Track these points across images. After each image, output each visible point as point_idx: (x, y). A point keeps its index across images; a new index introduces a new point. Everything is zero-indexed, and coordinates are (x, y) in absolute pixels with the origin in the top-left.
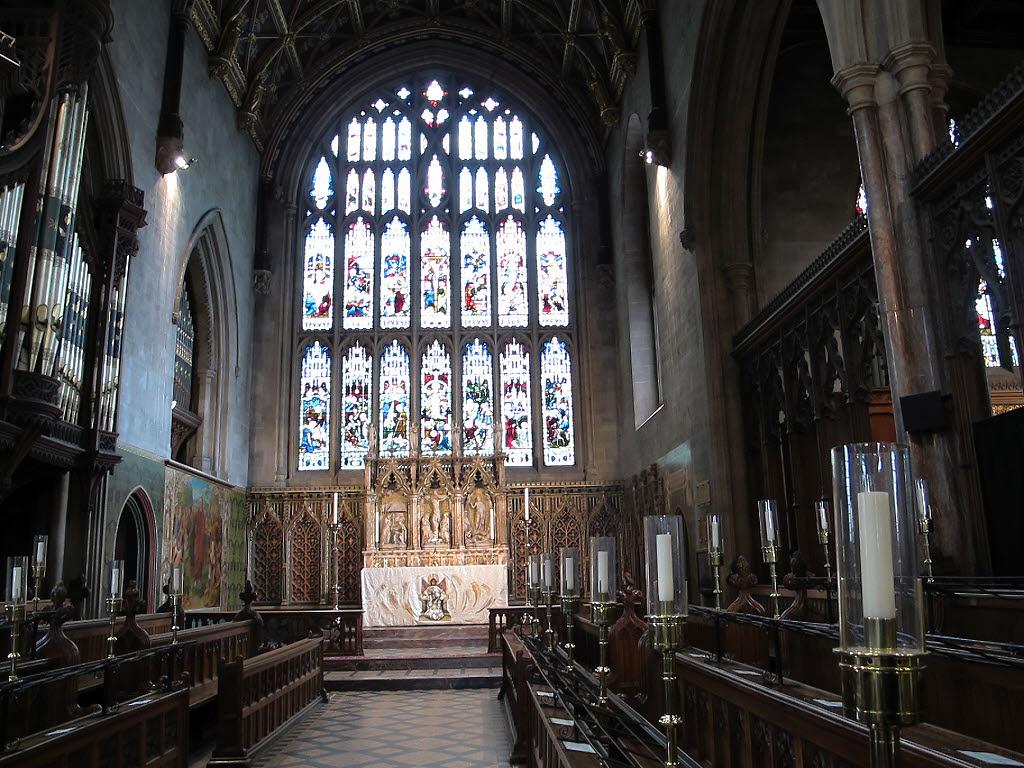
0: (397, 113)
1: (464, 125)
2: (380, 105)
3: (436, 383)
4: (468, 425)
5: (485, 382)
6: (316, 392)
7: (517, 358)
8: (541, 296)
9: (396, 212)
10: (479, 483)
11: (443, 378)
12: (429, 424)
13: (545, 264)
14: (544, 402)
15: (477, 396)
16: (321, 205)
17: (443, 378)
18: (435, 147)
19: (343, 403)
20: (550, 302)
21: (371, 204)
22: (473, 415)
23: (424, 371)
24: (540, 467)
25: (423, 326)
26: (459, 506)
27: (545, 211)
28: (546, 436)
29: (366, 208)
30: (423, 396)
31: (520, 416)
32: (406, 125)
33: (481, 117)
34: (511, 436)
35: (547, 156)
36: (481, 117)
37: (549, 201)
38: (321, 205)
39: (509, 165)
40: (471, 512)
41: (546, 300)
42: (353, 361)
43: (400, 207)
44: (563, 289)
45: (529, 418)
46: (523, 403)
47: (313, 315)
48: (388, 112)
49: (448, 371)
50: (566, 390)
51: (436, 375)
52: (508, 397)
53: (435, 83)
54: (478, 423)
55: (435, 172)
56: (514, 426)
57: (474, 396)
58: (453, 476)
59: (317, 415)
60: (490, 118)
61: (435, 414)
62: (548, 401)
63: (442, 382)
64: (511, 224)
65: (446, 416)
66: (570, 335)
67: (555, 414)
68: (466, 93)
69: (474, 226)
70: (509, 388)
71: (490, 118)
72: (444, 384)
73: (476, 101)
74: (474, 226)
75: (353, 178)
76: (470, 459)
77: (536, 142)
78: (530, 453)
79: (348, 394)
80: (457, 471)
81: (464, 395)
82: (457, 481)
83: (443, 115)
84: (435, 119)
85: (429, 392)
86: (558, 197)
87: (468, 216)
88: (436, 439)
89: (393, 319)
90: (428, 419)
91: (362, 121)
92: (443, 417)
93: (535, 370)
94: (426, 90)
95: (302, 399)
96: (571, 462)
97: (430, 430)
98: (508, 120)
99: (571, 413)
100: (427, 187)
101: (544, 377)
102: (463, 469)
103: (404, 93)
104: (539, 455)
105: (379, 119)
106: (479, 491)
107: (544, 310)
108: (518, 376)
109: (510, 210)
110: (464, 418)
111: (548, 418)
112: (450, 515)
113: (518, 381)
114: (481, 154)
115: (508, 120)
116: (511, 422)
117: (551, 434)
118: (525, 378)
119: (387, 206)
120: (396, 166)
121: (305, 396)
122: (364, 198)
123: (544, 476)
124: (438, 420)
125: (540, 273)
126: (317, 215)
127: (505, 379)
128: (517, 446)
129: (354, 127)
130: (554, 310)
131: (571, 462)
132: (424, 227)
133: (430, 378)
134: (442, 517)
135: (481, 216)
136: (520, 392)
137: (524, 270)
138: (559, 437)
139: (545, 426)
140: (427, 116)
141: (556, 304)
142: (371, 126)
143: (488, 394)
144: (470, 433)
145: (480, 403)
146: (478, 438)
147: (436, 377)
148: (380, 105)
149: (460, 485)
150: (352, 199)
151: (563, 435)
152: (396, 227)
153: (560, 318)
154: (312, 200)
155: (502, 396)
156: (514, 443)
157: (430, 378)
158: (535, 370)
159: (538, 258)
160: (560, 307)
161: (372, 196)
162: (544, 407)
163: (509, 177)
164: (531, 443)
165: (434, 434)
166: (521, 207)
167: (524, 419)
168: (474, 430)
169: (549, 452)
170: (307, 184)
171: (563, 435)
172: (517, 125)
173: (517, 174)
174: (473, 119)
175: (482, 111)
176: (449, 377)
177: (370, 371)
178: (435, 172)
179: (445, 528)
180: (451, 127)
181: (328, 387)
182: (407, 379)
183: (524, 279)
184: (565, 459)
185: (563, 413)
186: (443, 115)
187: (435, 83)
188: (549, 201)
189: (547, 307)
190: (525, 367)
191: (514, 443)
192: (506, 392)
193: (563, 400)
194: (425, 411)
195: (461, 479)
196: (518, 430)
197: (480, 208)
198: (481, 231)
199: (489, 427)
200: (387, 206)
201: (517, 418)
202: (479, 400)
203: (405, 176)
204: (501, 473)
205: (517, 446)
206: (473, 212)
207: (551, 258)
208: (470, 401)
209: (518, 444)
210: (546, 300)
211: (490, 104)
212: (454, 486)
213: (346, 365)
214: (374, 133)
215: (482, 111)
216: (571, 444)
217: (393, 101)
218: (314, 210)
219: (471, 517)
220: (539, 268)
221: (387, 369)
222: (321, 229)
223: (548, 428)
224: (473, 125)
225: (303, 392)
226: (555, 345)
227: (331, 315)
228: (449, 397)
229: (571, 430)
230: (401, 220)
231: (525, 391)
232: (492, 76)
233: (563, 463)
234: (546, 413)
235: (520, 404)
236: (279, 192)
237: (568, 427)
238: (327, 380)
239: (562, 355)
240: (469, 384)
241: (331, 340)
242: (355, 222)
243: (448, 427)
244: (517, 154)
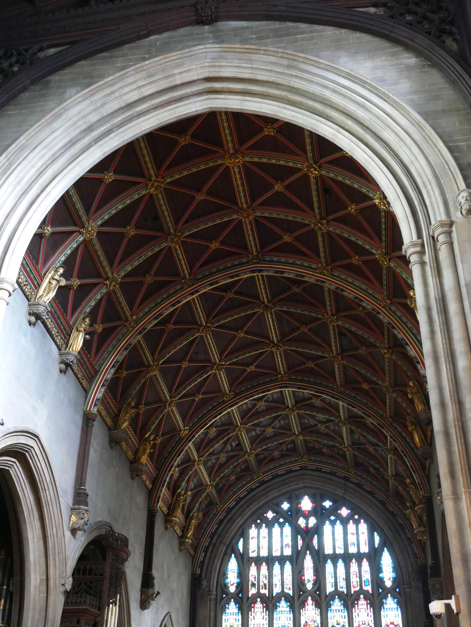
0: (281, 520)
1: (327, 528)
2: (270, 515)
9: (283, 594)
16: (232, 589)
18: (308, 546)
21: (266, 589)
29: (263, 591)
32: (287, 529)
33: (338, 522)
35: (385, 549)
36: (338, 522)
37: (388, 584)
38: (232, 589)
39: (359, 557)
43: (286, 591)
48: (275, 520)
53: (306, 497)
55: (308, 563)
60: (345, 522)
64: (362, 602)
68: (327, 504)
69: (337, 604)
71: (345, 522)
73: (334, 510)
74: (337, 604)
75: (253, 570)
77: (377, 539)
83: (312, 521)
84: (307, 524)
86: (395, 580)
87: (332, 597)
91: (258, 527)
94: (300, 503)
98: (357, 523)
100: (303, 575)
103: (285, 506)
105: (270, 525)
109: (361, 591)
114: (340, 551)
115: (357, 523)
119: (277, 590)
120: (282, 560)
122: (261, 584)
126: (230, 596)
129: (253, 532)
132: (303, 605)
135: (342, 596)
140: (302, 522)
142: (264, 531)
148: (270, 515)
150: (253, 585)
152: (283, 605)
154: (226, 586)
161: (266, 582)
163: (360, 566)
166: (368, 588)
170: (223, 574)
172: (363, 527)
173: (365, 564)
174: (333, 523)
175: (339, 517)
178: (308, 563)
180: (318, 530)
186: (312, 521)
187: (306, 497)
188: (388, 584)
197: (341, 590)
198: (342, 608)
200: (277, 590)
203: (288, 567)
206: (337, 593)
211: (344, 512)
214: (267, 535)
215: (339, 517)
217: (279, 512)
218: (228, 593)
222: (232, 608)
224: (333, 527)
230: (286, 601)
232: (344, 494)
236: (205, 583)
242: (255, 602)
244: (365, 549)
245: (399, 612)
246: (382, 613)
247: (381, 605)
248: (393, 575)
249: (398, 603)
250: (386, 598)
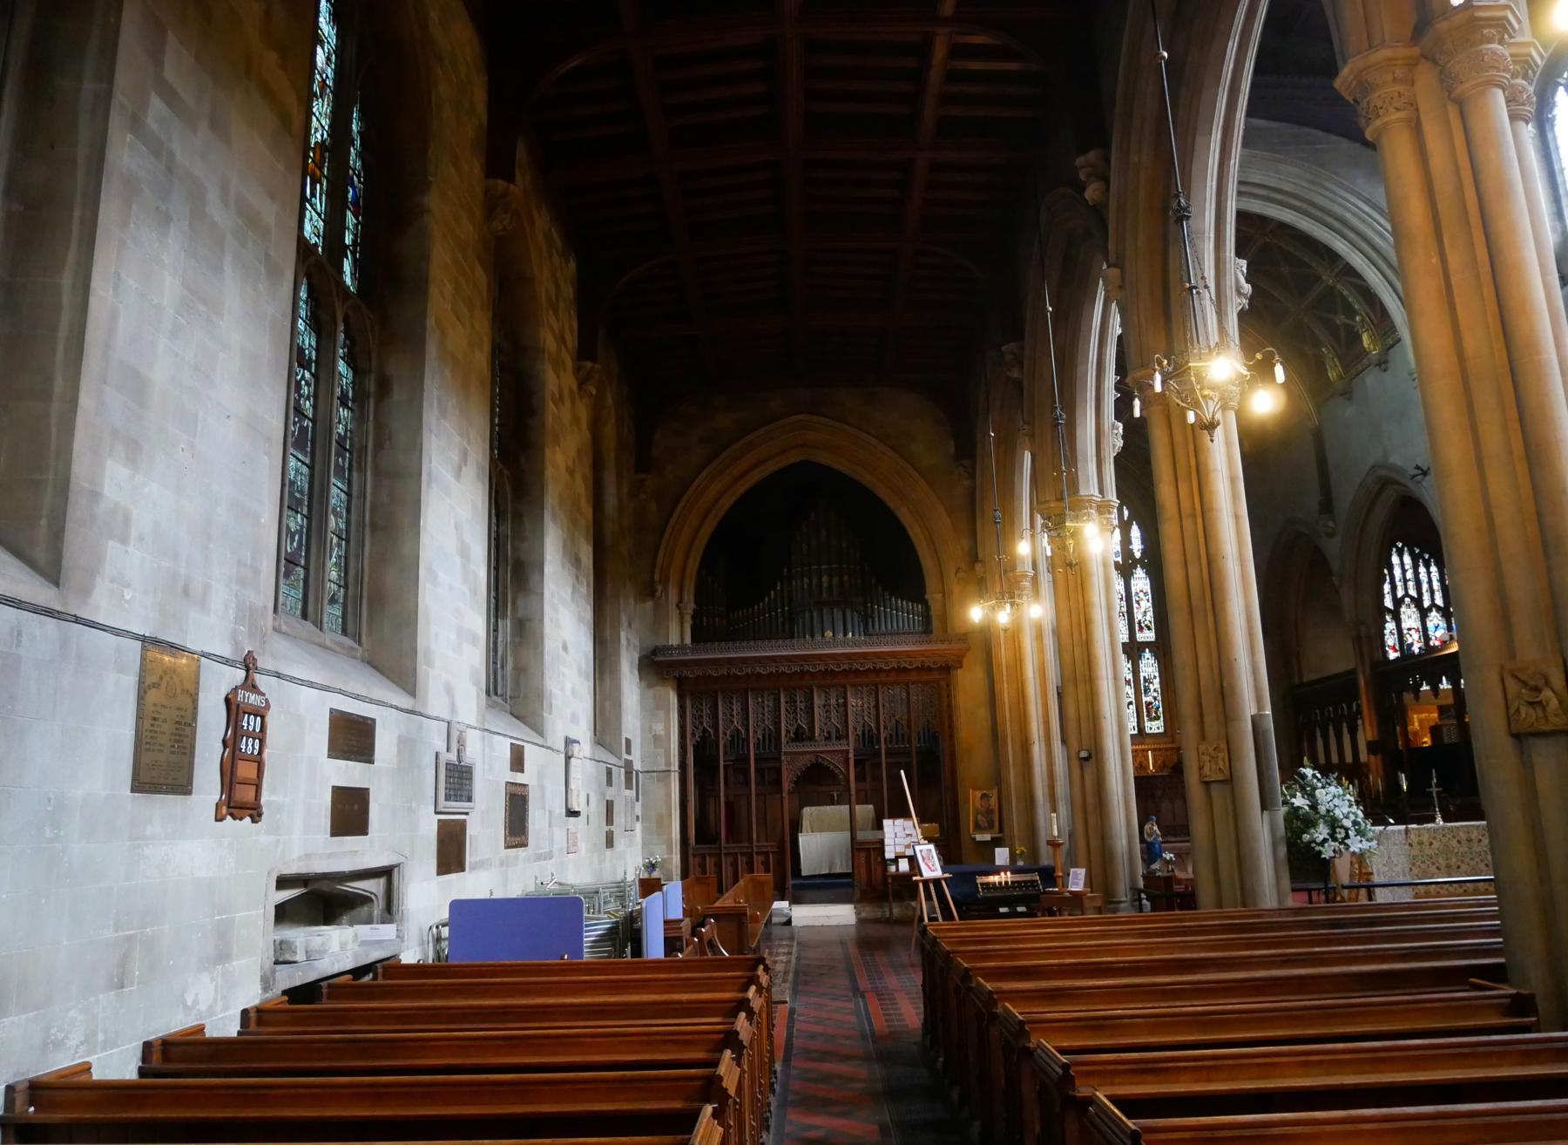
8: (1136, 621)
13: (1138, 599)
20: (1143, 625)
27: (1135, 562)
28: (1145, 714)
37: (1138, 555)
41: (1140, 623)
44: (1150, 616)
46: (1129, 693)
50: (1156, 684)
66: (1158, 648)
67: (1149, 699)
77: (1126, 513)
78: (1135, 724)
86: (1144, 552)
93: (1136, 671)
96: (1161, 730)
99: (1160, 698)
101: (1142, 675)
111: (1146, 702)
117: (1149, 715)
118: (1130, 677)
123: (1148, 740)
125: (1135, 605)
130: (1146, 630)
131: (1161, 730)
137: (1124, 603)
138: (1154, 714)
141: (1146, 626)
151: (1156, 713)
153: (1148, 636)
158: (1136, 671)
159: (1133, 595)
160: (1149, 628)
162: (1143, 695)
169: (1148, 724)
171: (1156, 713)
183: (1124, 609)
184: (1158, 728)
185: (1155, 698)
188: (1138, 555)
189: (1141, 629)
190: (1129, 669)
193: (1155, 690)
207: (1141, 595)
210: (1140, 623)
216: (1162, 719)
220: (1134, 602)
226: (1147, 654)
229: (1161, 709)
233: (1157, 731)
234: (1145, 699)
237: (1159, 707)
239: (1152, 661)
245: (1148, 581)
246: (1132, 582)
247: (1132, 574)
248: (1141, 547)
249: (1146, 573)
250: (1136, 568)
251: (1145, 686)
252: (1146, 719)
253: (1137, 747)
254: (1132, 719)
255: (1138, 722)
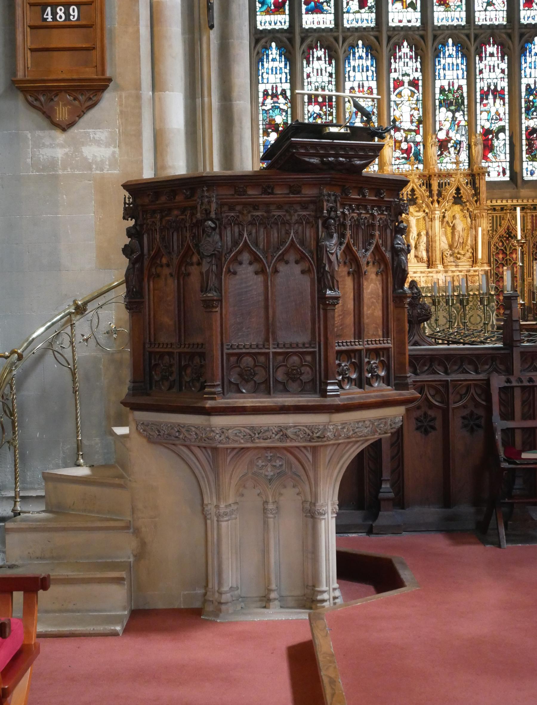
3: (406, 90)
4: (442, 135)
5: (460, 87)
6: (275, 99)
7: (494, 61)
10: (458, 199)
11: (414, 83)
12: (399, 136)
14: (523, 110)
15: (451, 104)
17: (414, 83)
19: (306, 112)
22: (447, 125)
23: (393, 75)
24: (519, 181)
25: (391, 24)
26: (437, 223)
28: (524, 148)
30: (392, 104)
31: (497, 125)
34: (488, 147)
40: (449, 230)
42: (317, 64)
45: (507, 128)
46: (501, 111)
47: (268, 12)
49: (418, 75)
51: (406, 79)
52: (485, 105)
54: (452, 134)
56: (490, 136)
57: (446, 104)
58: (431, 191)
59: (278, 125)
61: (406, 125)
62: (528, 109)
63: (413, 89)
65: (418, 126)
70: (485, 95)
72: (416, 91)
76: (449, 175)
78: (507, 165)
79: (310, 103)
80: (435, 187)
81: (437, 103)
82: (435, 198)
85: (398, 100)
88: (407, 151)
89: (358, 16)
90: (398, 129)
92: (414, 128)
95: (260, 108)
97: (401, 142)
101: (524, 81)
102: (440, 185)
104: (517, 169)
106: (457, 208)
107: (525, 5)
108: (495, 81)
110: (438, 128)
111: (527, 128)
112: (427, 234)
113: (496, 87)
116: (487, 132)
118: (504, 84)
121: (263, 104)
123: (524, 192)
124: (410, 130)
127: (480, 85)
128: (494, 160)
133: (399, 83)
134: (419, 235)
136: (498, 101)
139: (524, 137)
143: (463, 103)
144: (443, 145)
145: (454, 112)
146: (452, 150)
147: (406, 84)
149: (438, 202)
155: (478, 105)
156: (490, 155)
157: (399, 83)
162: (523, 116)
164: (508, 156)
165: (404, 146)
167: (502, 129)
168: (448, 140)
176: (420, 83)
177: (334, 76)
179: (423, 247)
181: (288, 94)
182: (374, 85)
190: (503, 71)
191: (490, 155)
192: (482, 99)
194: (394, 121)
195: (440, 194)
196: (496, 143)
199: (463, 139)
201: (494, 127)
202: (453, 108)
204: (483, 188)
205: (494, 160)
208: (443, 109)
209: (495, 156)
212: (432, 203)
213: (307, 70)
219: (449, 235)
221: (352, 74)
223: (527, 139)
225: (261, 100)
227: (287, 12)
228: (420, 106)
231: (503, 99)
235: (497, 113)
238: (287, 86)
240: (442, 90)
241: (291, 40)
243: (419, 138)
251: (527, 101)
252: (525, 155)
253: (504, 202)
254: (502, 157)
255: (512, 162)
